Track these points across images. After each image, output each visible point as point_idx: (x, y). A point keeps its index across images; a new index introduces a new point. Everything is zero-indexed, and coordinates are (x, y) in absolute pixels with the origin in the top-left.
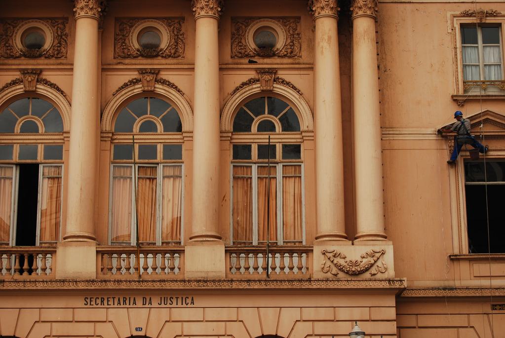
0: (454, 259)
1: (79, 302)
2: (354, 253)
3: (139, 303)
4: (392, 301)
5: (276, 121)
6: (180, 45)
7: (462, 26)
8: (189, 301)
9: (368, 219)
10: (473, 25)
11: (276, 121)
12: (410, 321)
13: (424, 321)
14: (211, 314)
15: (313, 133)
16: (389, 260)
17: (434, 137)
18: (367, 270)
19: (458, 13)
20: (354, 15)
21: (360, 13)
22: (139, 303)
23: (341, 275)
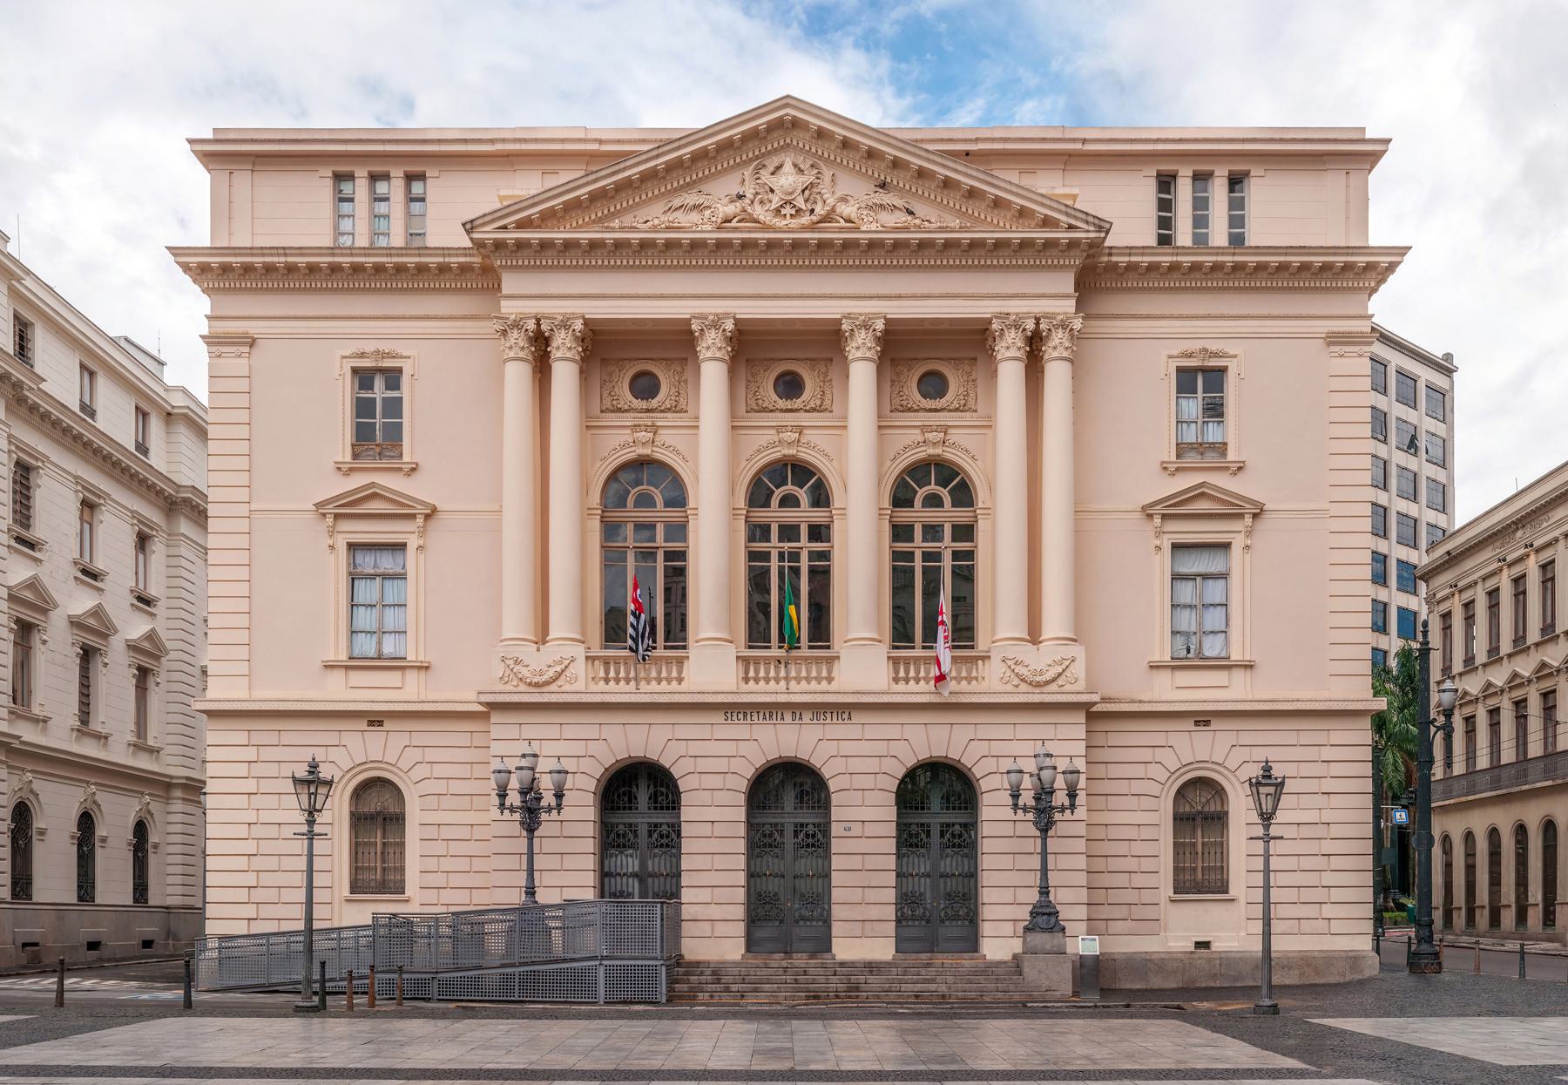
0: (1154, 667)
1: (718, 718)
2: (1040, 660)
3: (788, 717)
4: (1081, 717)
5: (944, 493)
6: (828, 396)
7: (1180, 370)
8: (845, 716)
9: (1055, 620)
10: (1196, 370)
11: (944, 493)
12: (1099, 739)
13: (1114, 739)
14: (870, 732)
15: (990, 511)
16: (1079, 669)
17: (1137, 515)
18: (1054, 680)
19: (1175, 353)
20: (1046, 357)
21: (1055, 354)
22: (788, 717)
23: (1024, 687)
